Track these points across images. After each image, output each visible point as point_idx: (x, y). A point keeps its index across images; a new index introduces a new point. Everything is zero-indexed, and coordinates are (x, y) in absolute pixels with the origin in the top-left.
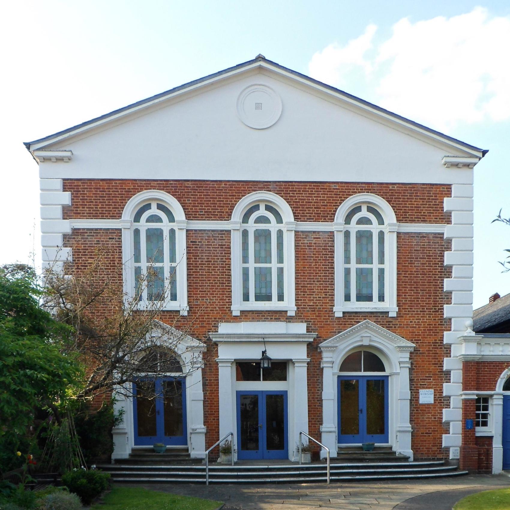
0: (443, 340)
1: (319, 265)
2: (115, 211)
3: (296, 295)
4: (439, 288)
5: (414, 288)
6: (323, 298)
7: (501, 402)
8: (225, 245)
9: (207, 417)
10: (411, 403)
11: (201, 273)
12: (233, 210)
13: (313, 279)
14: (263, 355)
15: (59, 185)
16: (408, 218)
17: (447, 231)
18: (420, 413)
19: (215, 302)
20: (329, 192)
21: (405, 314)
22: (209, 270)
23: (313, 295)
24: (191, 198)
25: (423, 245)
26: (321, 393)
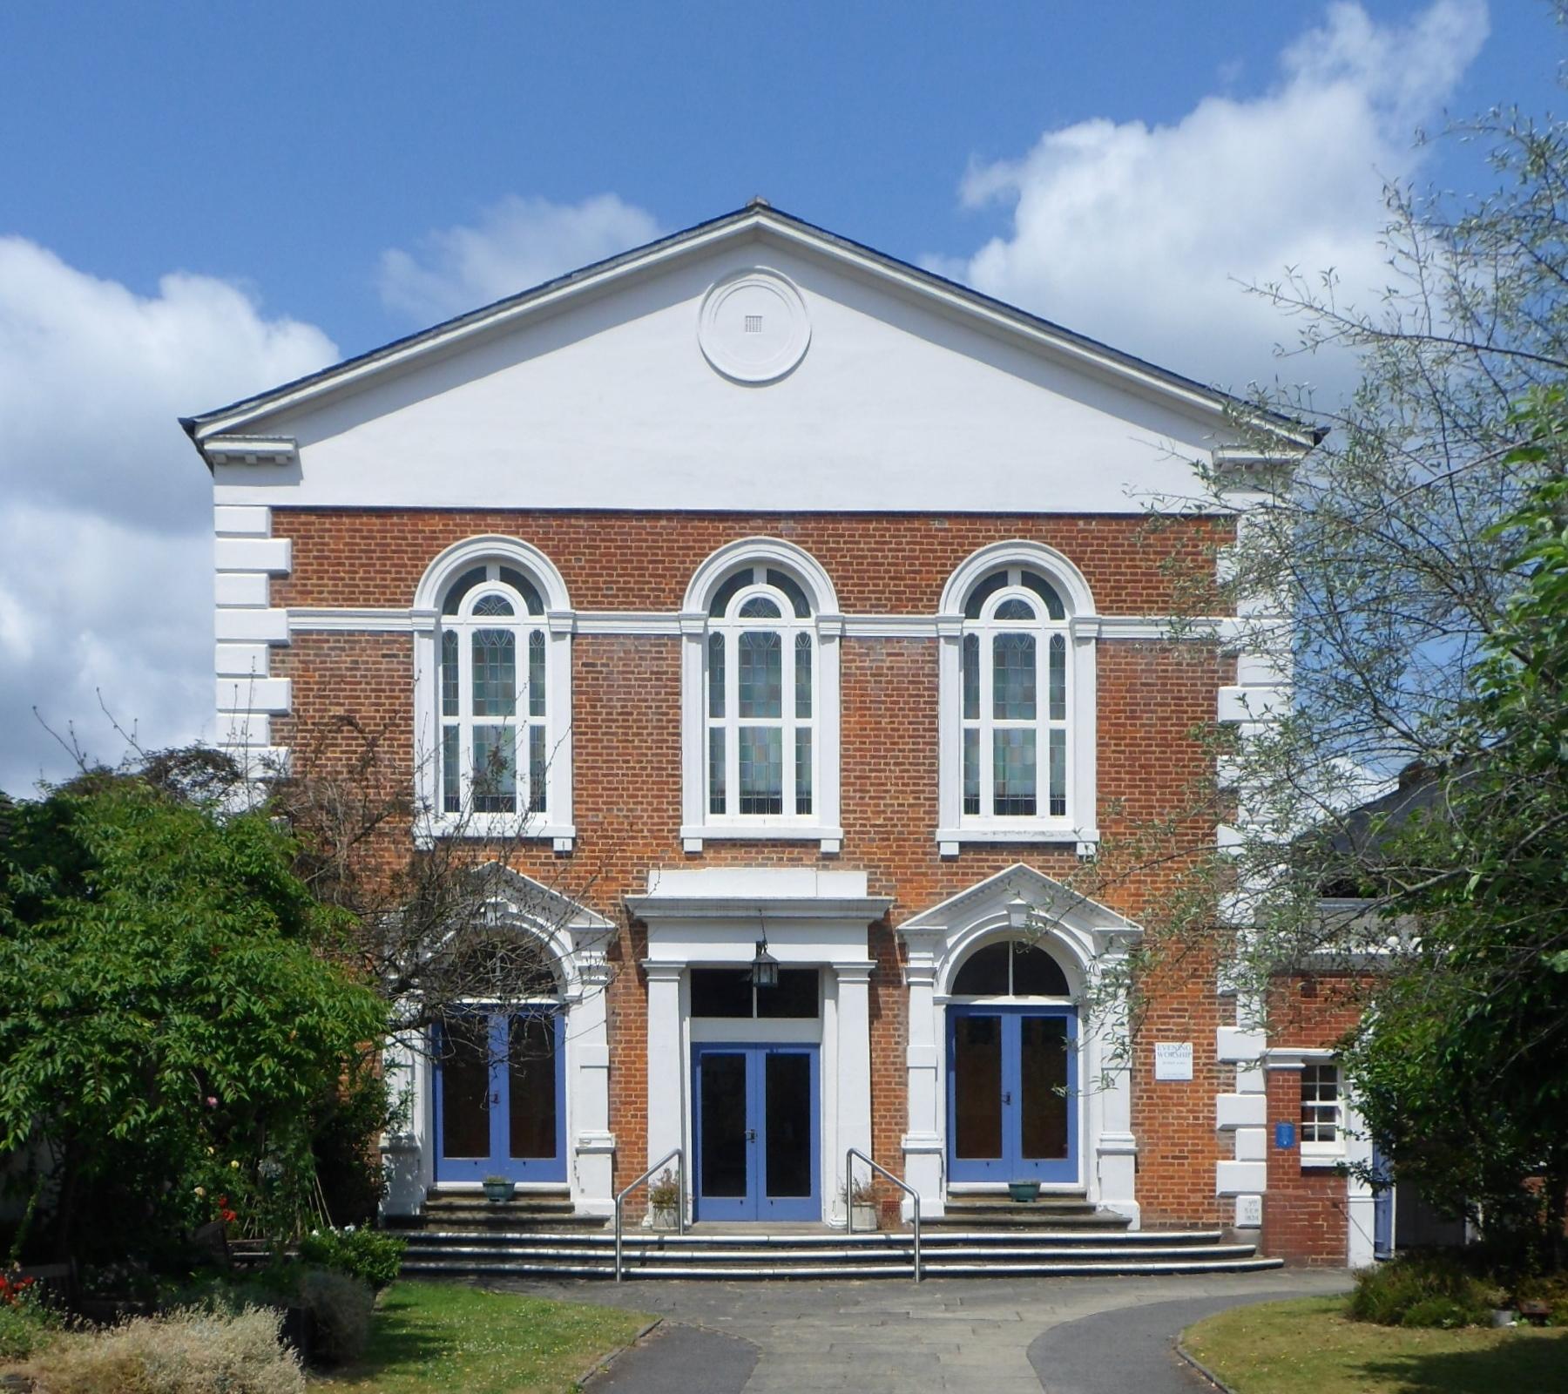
3: (842, 798)
6: (910, 805)
10: (1132, 1078)
14: (758, 953)
20: (926, 537)
22: (626, 734)
26: (905, 1050)
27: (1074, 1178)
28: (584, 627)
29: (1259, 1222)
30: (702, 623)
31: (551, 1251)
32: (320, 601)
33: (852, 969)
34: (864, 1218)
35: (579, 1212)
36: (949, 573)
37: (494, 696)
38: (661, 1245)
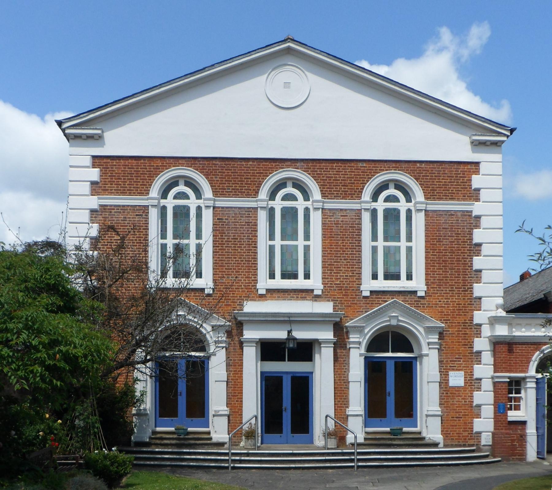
0: (473, 320)
1: (346, 243)
2: (143, 188)
3: (323, 273)
4: (469, 266)
5: (443, 266)
6: (350, 276)
7: (534, 385)
8: (251, 222)
9: (231, 399)
10: (440, 386)
11: (227, 251)
12: (260, 187)
13: (340, 257)
14: (288, 335)
15: (88, 161)
16: (436, 195)
17: (477, 208)
18: (450, 396)
19: (241, 280)
21: (433, 293)
23: (340, 273)
24: (218, 175)
25: (451, 223)
26: (348, 375)
27: (416, 426)
28: (218, 204)
29: (491, 444)
30: (266, 203)
31: (202, 457)
32: (111, 193)
33: (327, 341)
34: (332, 443)
35: (214, 440)
36: (366, 184)
37: (181, 232)
38: (248, 455)
